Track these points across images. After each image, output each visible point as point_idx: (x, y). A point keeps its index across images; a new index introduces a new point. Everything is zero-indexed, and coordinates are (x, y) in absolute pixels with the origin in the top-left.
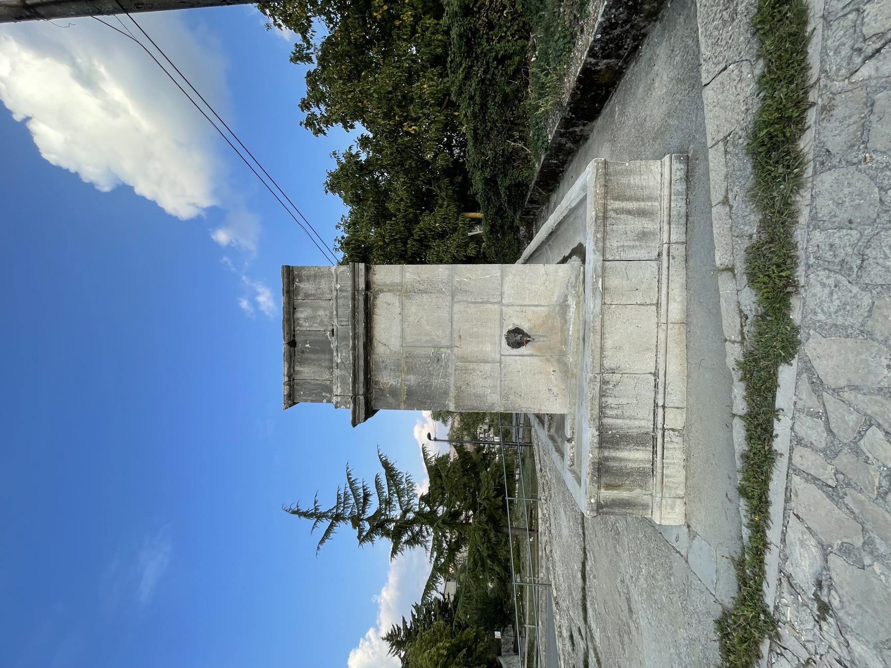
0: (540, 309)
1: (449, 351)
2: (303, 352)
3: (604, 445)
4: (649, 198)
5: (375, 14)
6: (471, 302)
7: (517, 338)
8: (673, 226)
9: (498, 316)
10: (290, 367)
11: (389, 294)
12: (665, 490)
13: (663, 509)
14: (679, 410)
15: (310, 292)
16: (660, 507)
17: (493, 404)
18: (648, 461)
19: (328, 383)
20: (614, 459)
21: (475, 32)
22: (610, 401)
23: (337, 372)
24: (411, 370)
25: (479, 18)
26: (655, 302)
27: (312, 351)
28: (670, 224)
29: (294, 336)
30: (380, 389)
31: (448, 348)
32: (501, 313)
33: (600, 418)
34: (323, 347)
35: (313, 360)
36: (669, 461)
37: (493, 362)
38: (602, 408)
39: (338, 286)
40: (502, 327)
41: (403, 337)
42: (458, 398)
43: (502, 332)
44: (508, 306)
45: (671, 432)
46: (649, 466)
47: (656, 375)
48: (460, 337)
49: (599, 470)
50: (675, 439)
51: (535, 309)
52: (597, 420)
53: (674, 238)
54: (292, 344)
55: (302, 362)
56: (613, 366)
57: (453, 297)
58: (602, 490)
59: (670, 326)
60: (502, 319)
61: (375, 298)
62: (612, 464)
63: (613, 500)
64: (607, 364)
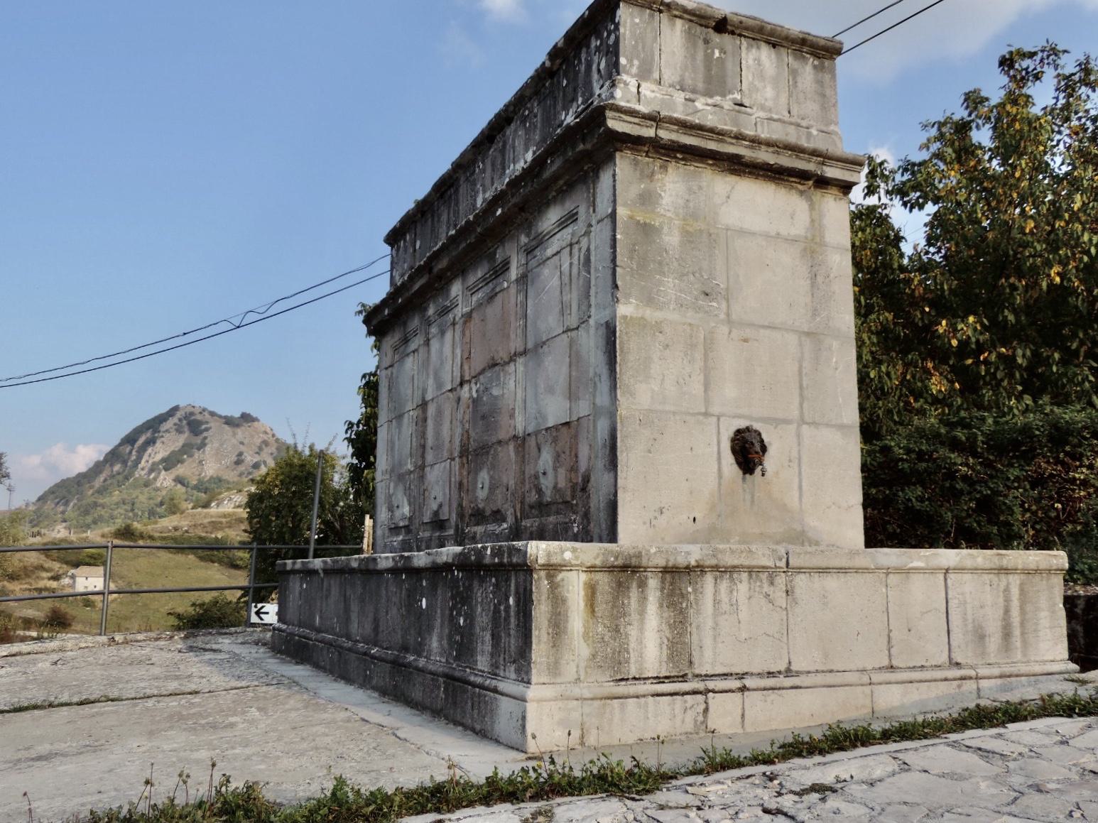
0: (796, 494)
1: (722, 316)
2: (706, 42)
3: (668, 576)
4: (1025, 643)
5: (944, 322)
6: (800, 368)
7: (748, 452)
8: (999, 681)
9: (780, 415)
10: (685, 10)
11: (808, 220)
12: (597, 703)
13: (560, 704)
14: (739, 719)
15: (799, 79)
16: (563, 697)
17: (632, 394)
18: (641, 669)
19: (656, 75)
20: (643, 600)
21: (1028, 457)
22: (743, 587)
23: (679, 97)
24: (689, 237)
25: (1048, 462)
26: (895, 663)
27: (708, 58)
28: (1001, 677)
29: (733, 33)
30: (653, 174)
31: (728, 315)
32: (787, 422)
33: (716, 568)
34: (715, 83)
35: (693, 58)
36: (651, 708)
37: (707, 401)
38: (731, 571)
39: (814, 132)
40: (766, 420)
41: (742, 232)
42: (642, 323)
43: (758, 420)
44: (799, 435)
45: (703, 706)
46: (633, 672)
47: (788, 672)
48: (746, 340)
49: (624, 568)
50: (690, 715)
51: (796, 486)
52: (714, 562)
53: (984, 684)
54: (722, 26)
55: (689, 35)
56: (798, 591)
57: (808, 334)
58: (584, 577)
59: (867, 689)
60: (776, 422)
61: (802, 193)
62: (634, 593)
63: (564, 601)
64: (801, 581)
